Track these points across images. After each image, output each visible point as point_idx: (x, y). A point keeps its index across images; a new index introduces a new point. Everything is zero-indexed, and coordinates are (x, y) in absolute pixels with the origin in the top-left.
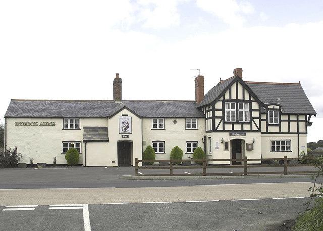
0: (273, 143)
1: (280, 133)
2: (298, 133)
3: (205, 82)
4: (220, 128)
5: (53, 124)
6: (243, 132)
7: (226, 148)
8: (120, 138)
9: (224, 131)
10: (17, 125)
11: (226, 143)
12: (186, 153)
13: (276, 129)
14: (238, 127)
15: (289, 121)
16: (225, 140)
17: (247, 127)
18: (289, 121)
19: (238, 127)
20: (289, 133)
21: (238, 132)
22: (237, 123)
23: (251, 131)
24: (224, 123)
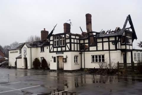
0: (93, 57)
1: (97, 50)
2: (109, 50)
3: (92, 18)
4: (52, 50)
5: (17, 52)
6: (62, 52)
7: (55, 61)
8: (24, 57)
9: (53, 52)
10: (11, 53)
11: (55, 58)
12: (92, 63)
13: (94, 48)
14: (59, 49)
15: (103, 42)
16: (54, 56)
17: (64, 49)
18: (103, 42)
19: (59, 49)
20: (103, 50)
21: (59, 52)
22: (59, 47)
23: (66, 51)
24: (54, 47)
